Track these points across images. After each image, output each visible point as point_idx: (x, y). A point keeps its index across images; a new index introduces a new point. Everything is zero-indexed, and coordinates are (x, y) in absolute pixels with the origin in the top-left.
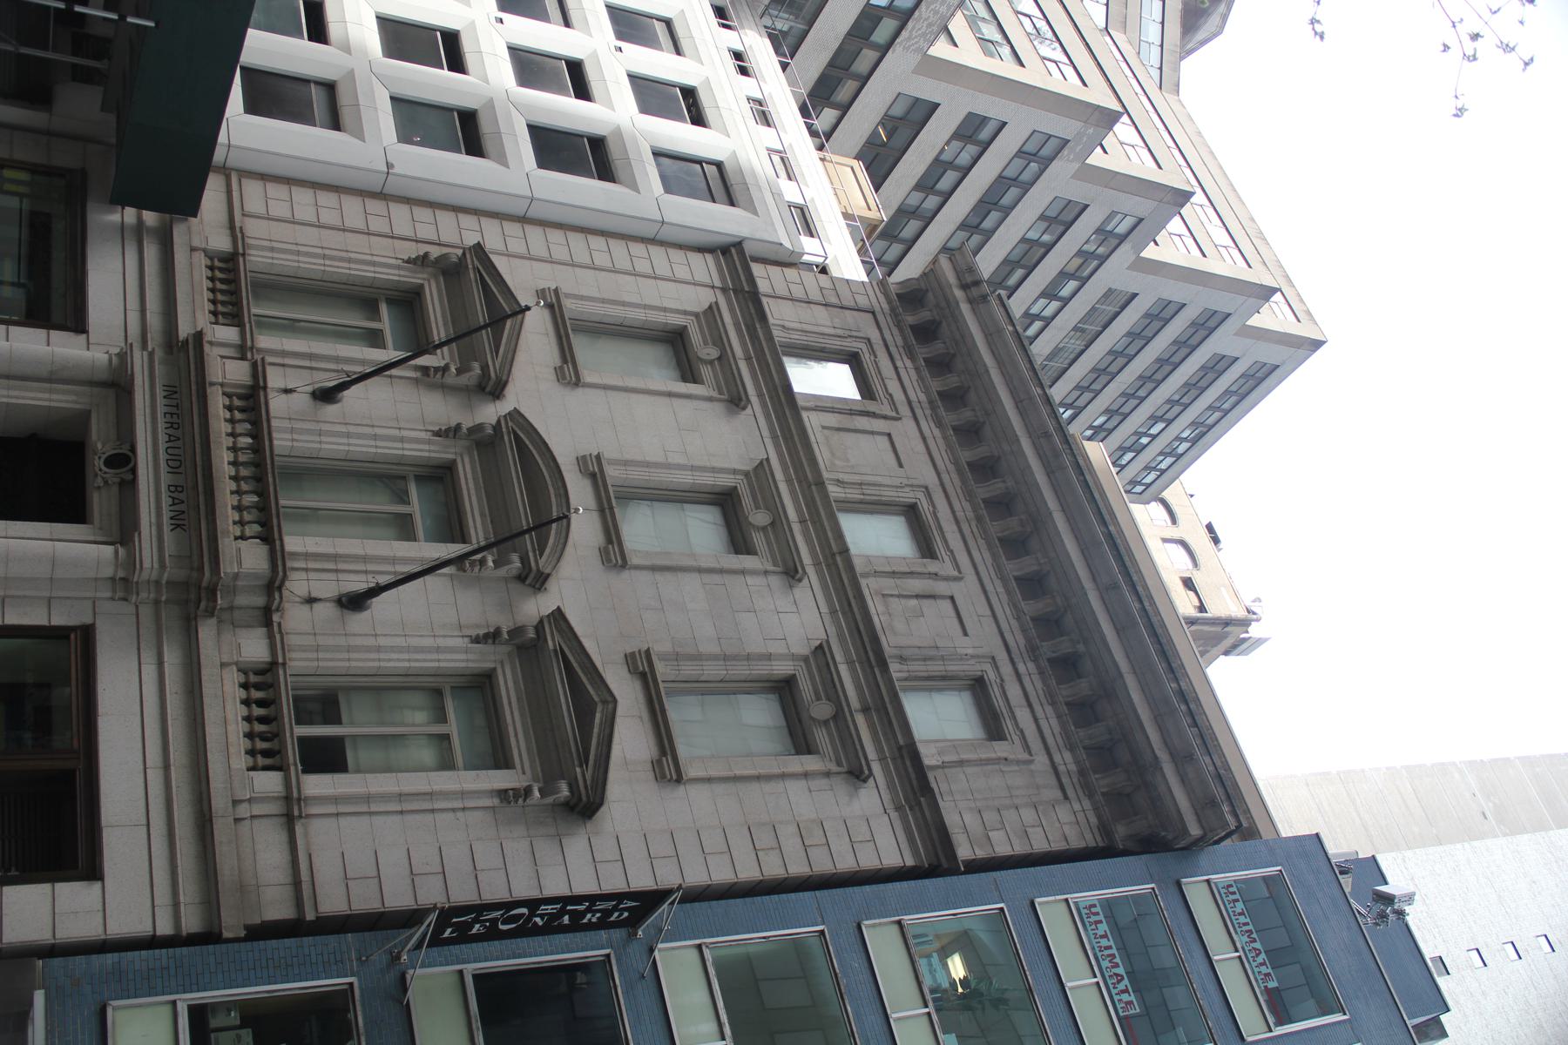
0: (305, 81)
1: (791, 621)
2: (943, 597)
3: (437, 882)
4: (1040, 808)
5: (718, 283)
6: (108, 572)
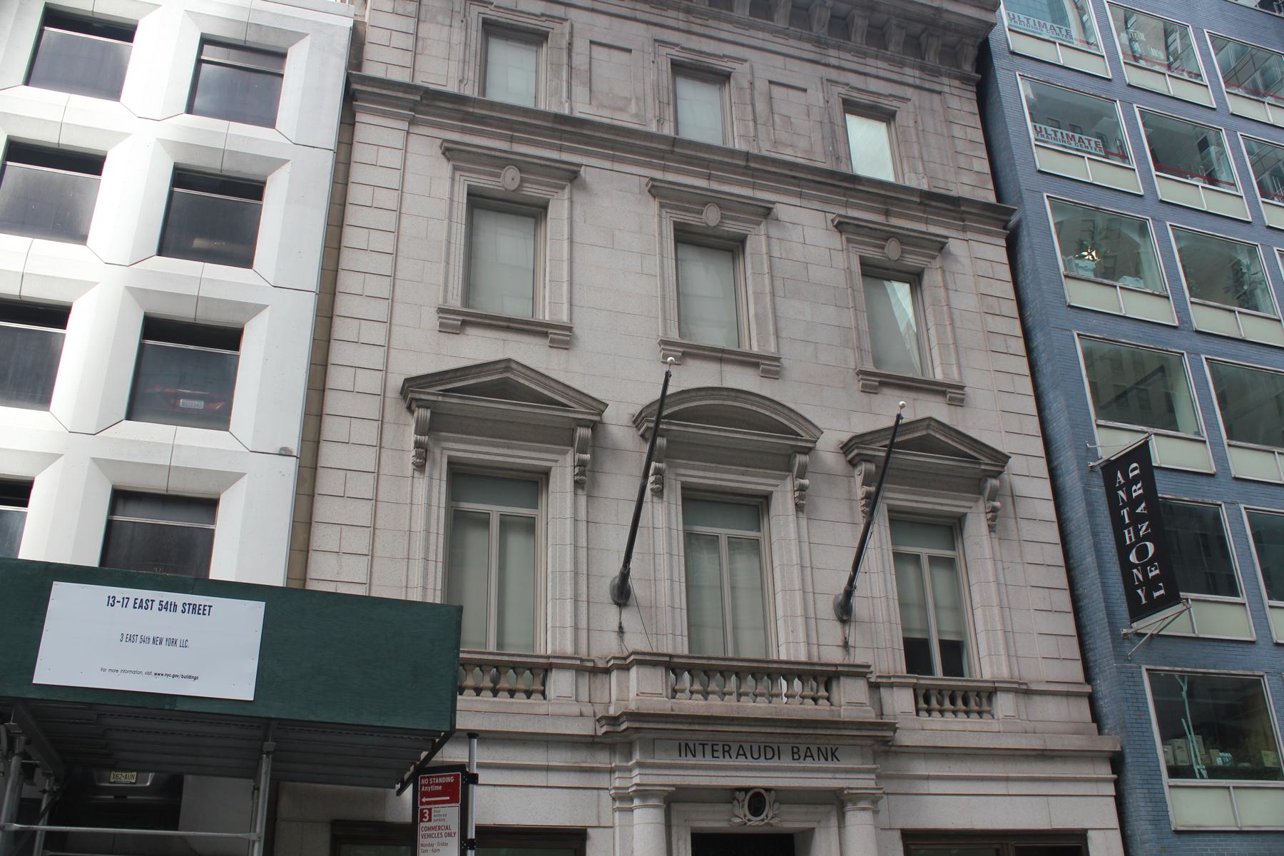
0: (111, 528)
1: (805, 237)
4: (951, 119)
5: (405, 125)
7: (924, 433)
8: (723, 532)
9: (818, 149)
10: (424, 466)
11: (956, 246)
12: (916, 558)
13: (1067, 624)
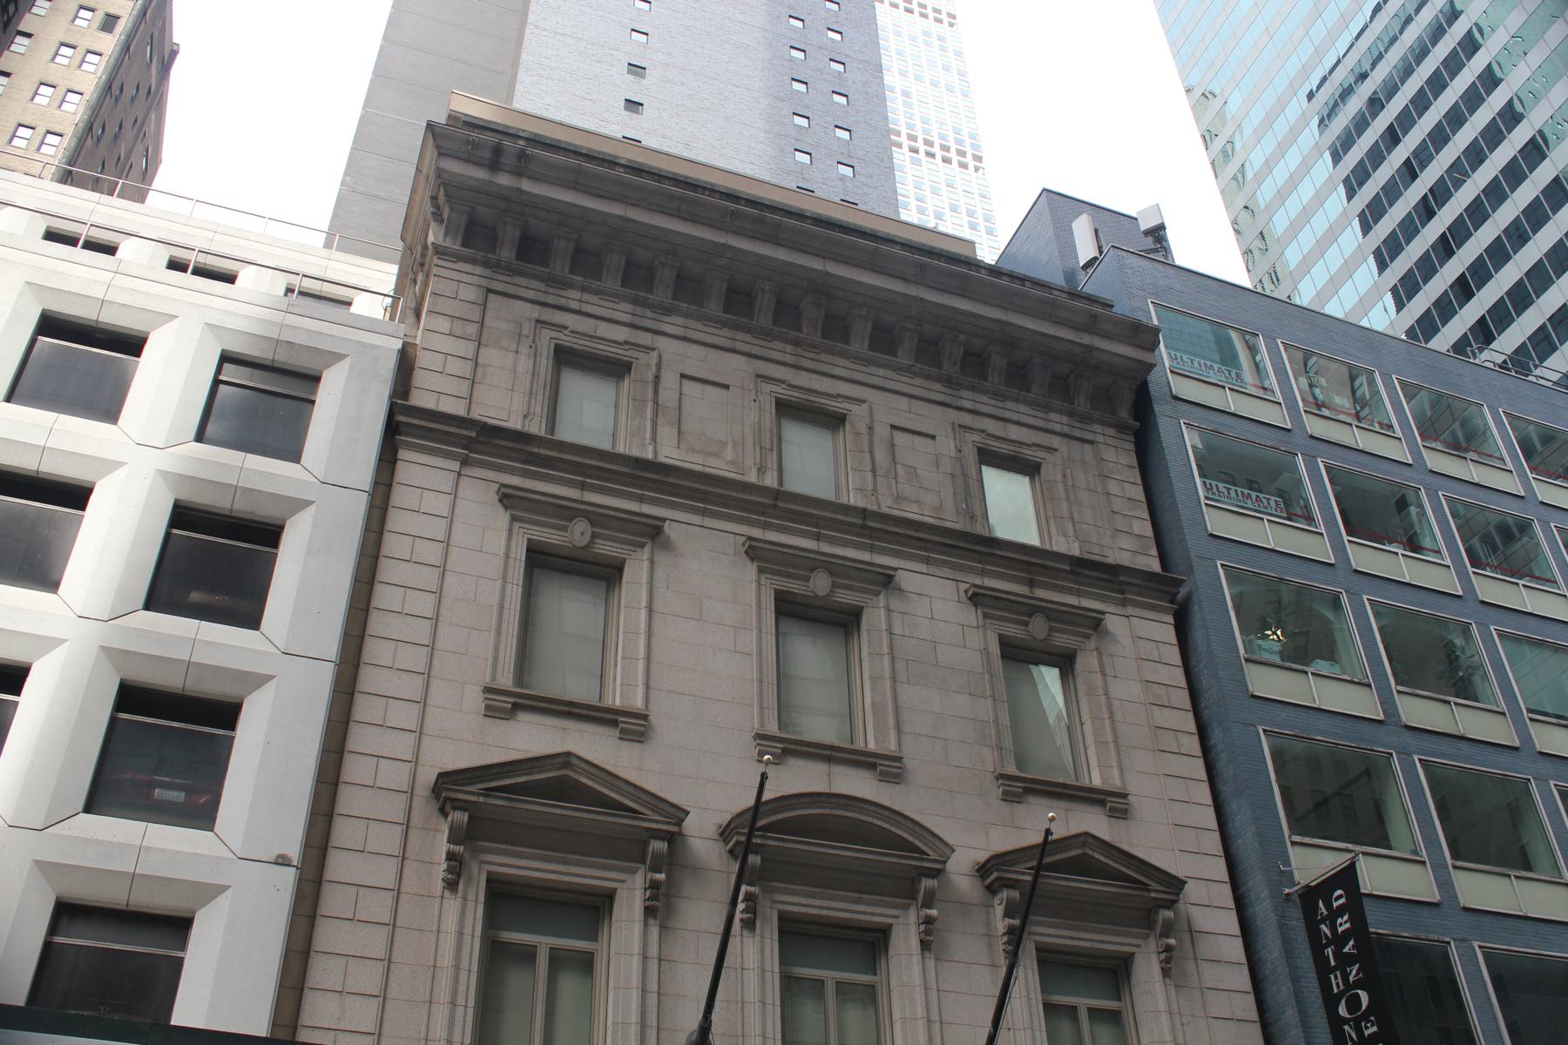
1: (932, 612)
5: (456, 466)
7: (1079, 851)
8: (830, 976)
9: (949, 505)
10: (457, 883)
11: (1115, 623)
12: (1072, 1011)
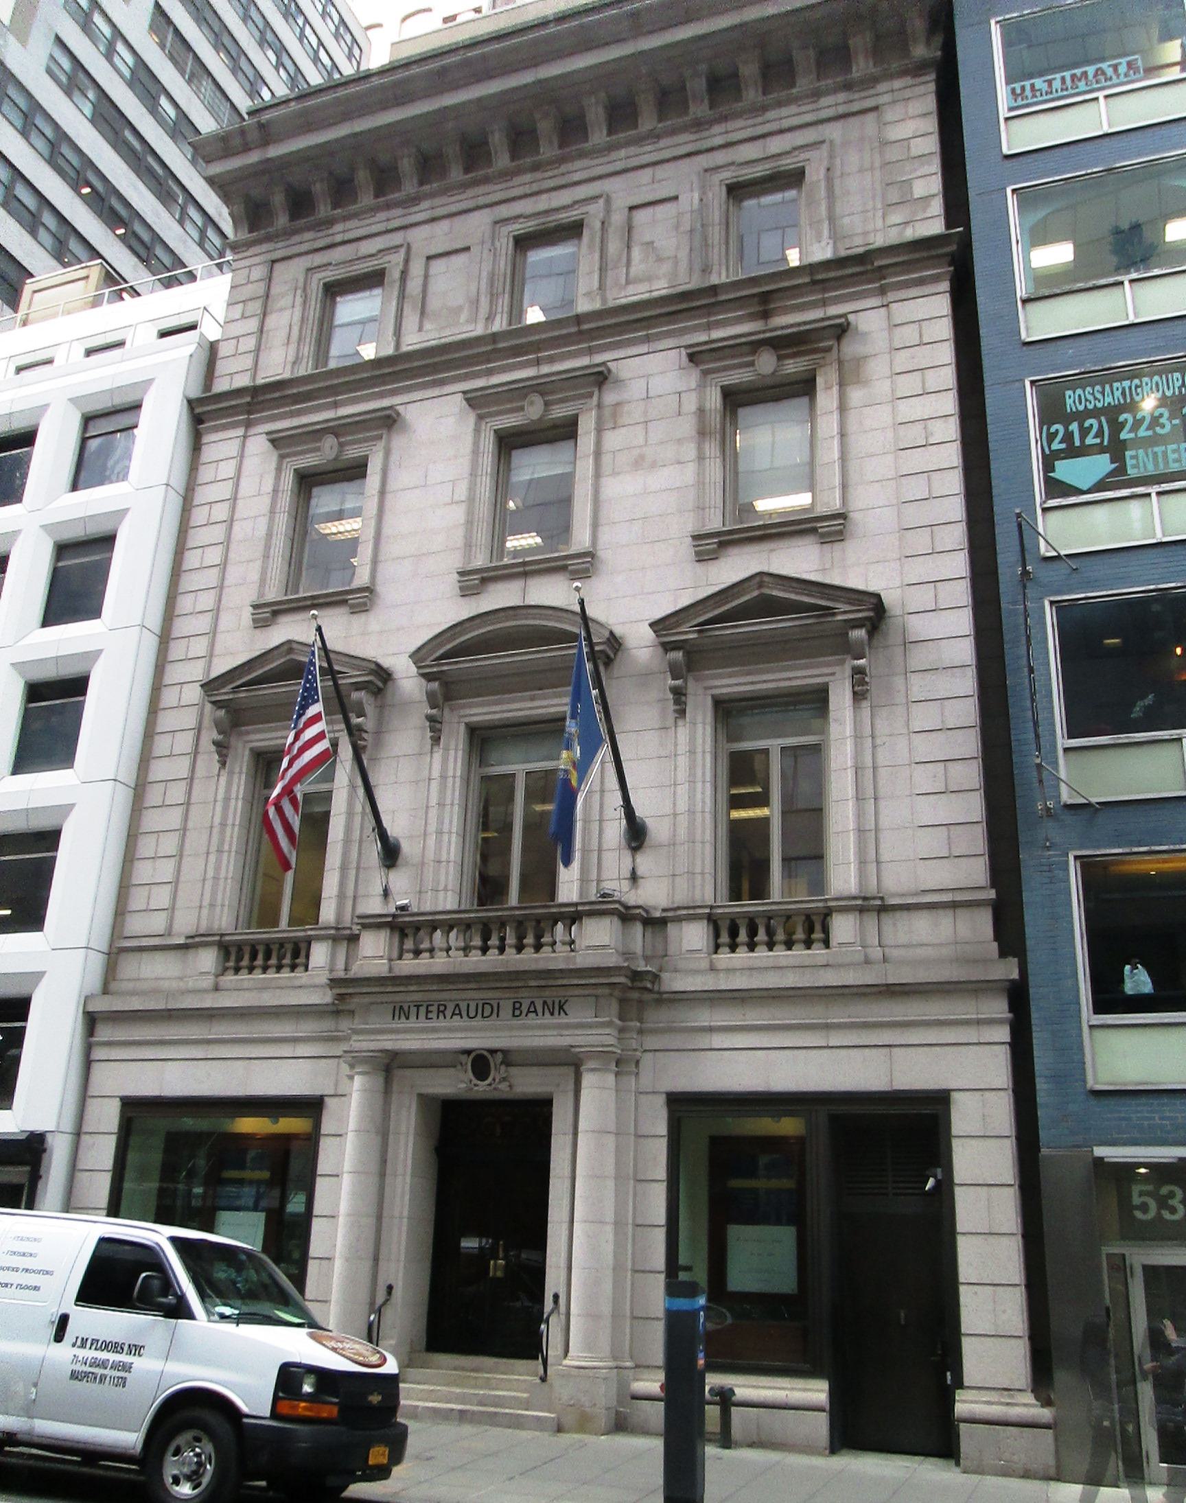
2: (630, 219)
3: (955, 768)
5: (240, 432)
6: (611, 1078)
7: (756, 593)
11: (870, 319)
13: (974, 807)
